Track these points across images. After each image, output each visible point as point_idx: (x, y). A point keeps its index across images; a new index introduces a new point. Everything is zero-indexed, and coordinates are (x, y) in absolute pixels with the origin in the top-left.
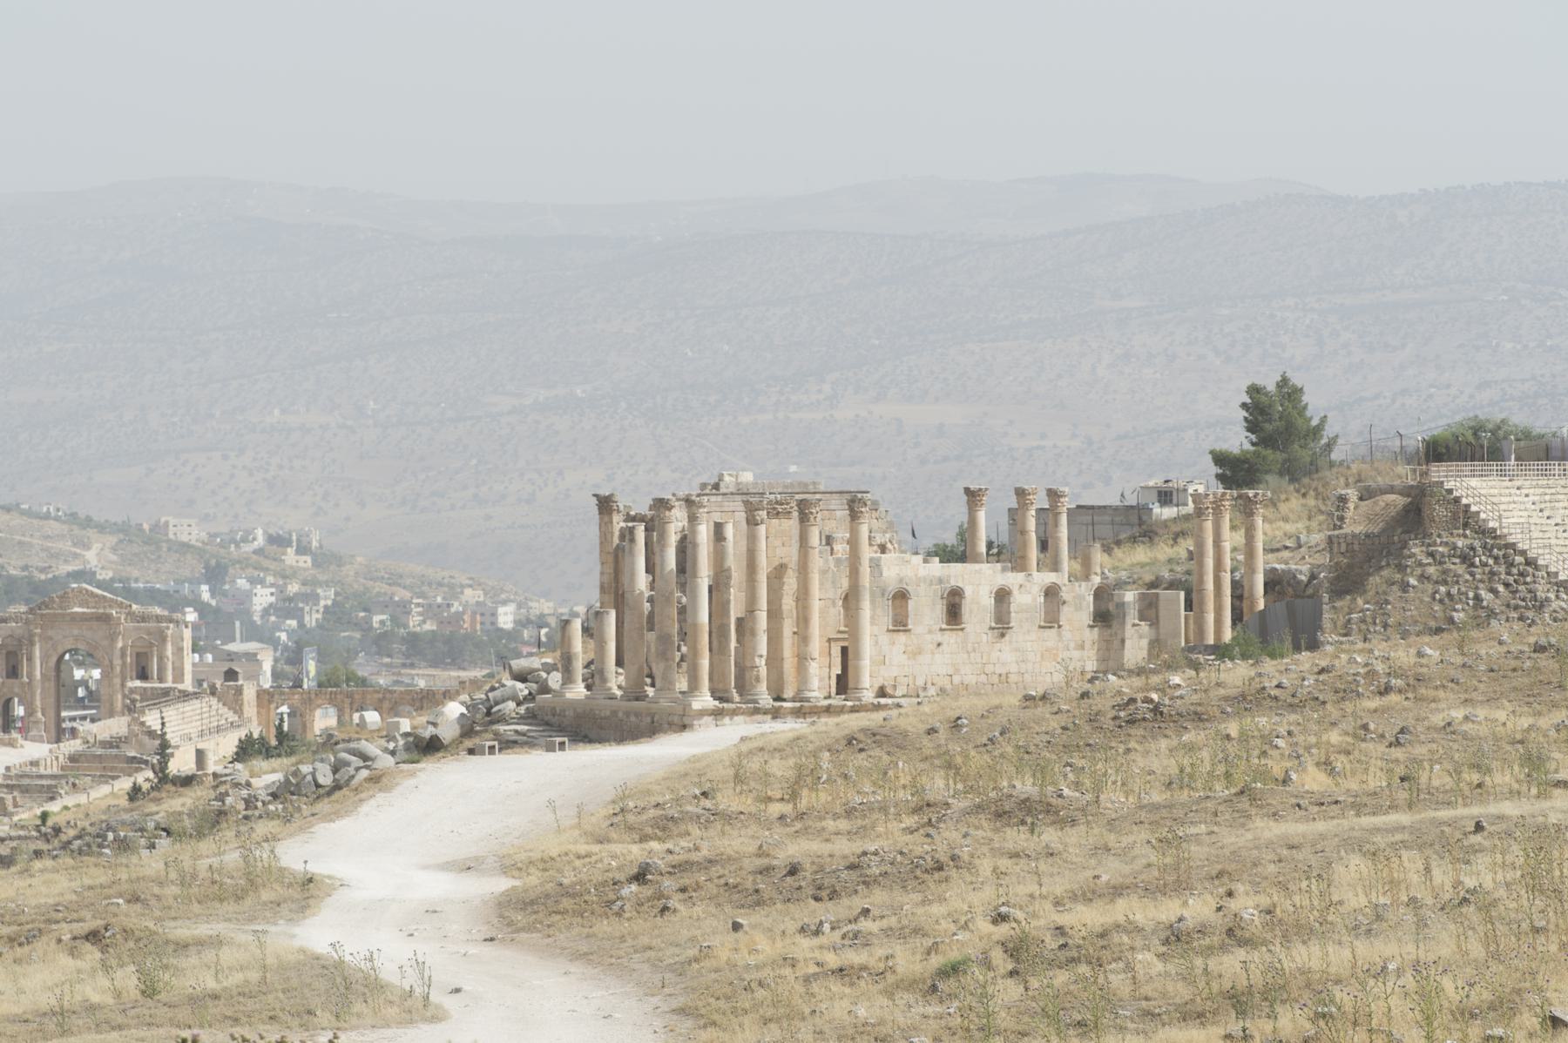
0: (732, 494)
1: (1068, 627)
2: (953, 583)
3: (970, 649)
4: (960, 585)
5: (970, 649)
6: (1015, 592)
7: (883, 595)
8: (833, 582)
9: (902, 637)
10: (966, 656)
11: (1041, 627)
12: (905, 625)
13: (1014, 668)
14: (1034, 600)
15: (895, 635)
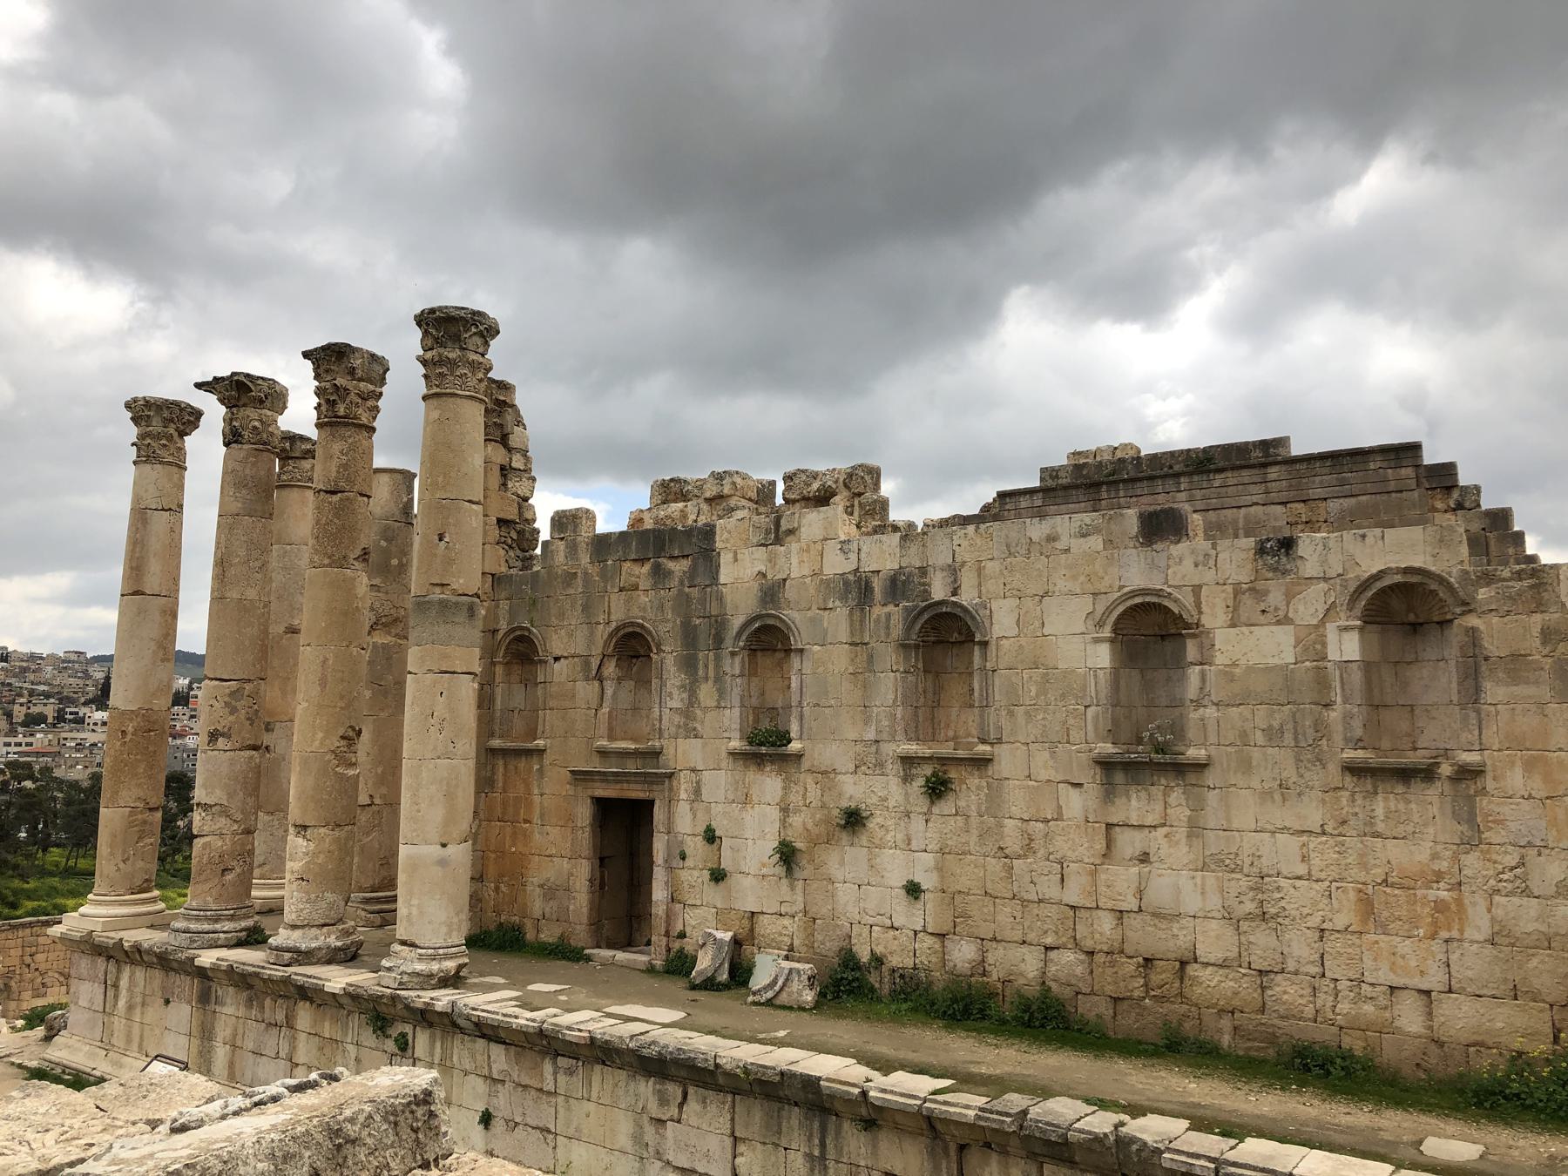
0: (1065, 488)
1: (1516, 779)
2: (939, 592)
3: (1013, 843)
4: (967, 597)
5: (1013, 843)
6: (1214, 617)
7: (718, 641)
8: (586, 608)
9: (769, 784)
10: (995, 866)
11: (1355, 770)
12: (785, 739)
13: (1213, 942)
14: (1311, 645)
15: (752, 775)
